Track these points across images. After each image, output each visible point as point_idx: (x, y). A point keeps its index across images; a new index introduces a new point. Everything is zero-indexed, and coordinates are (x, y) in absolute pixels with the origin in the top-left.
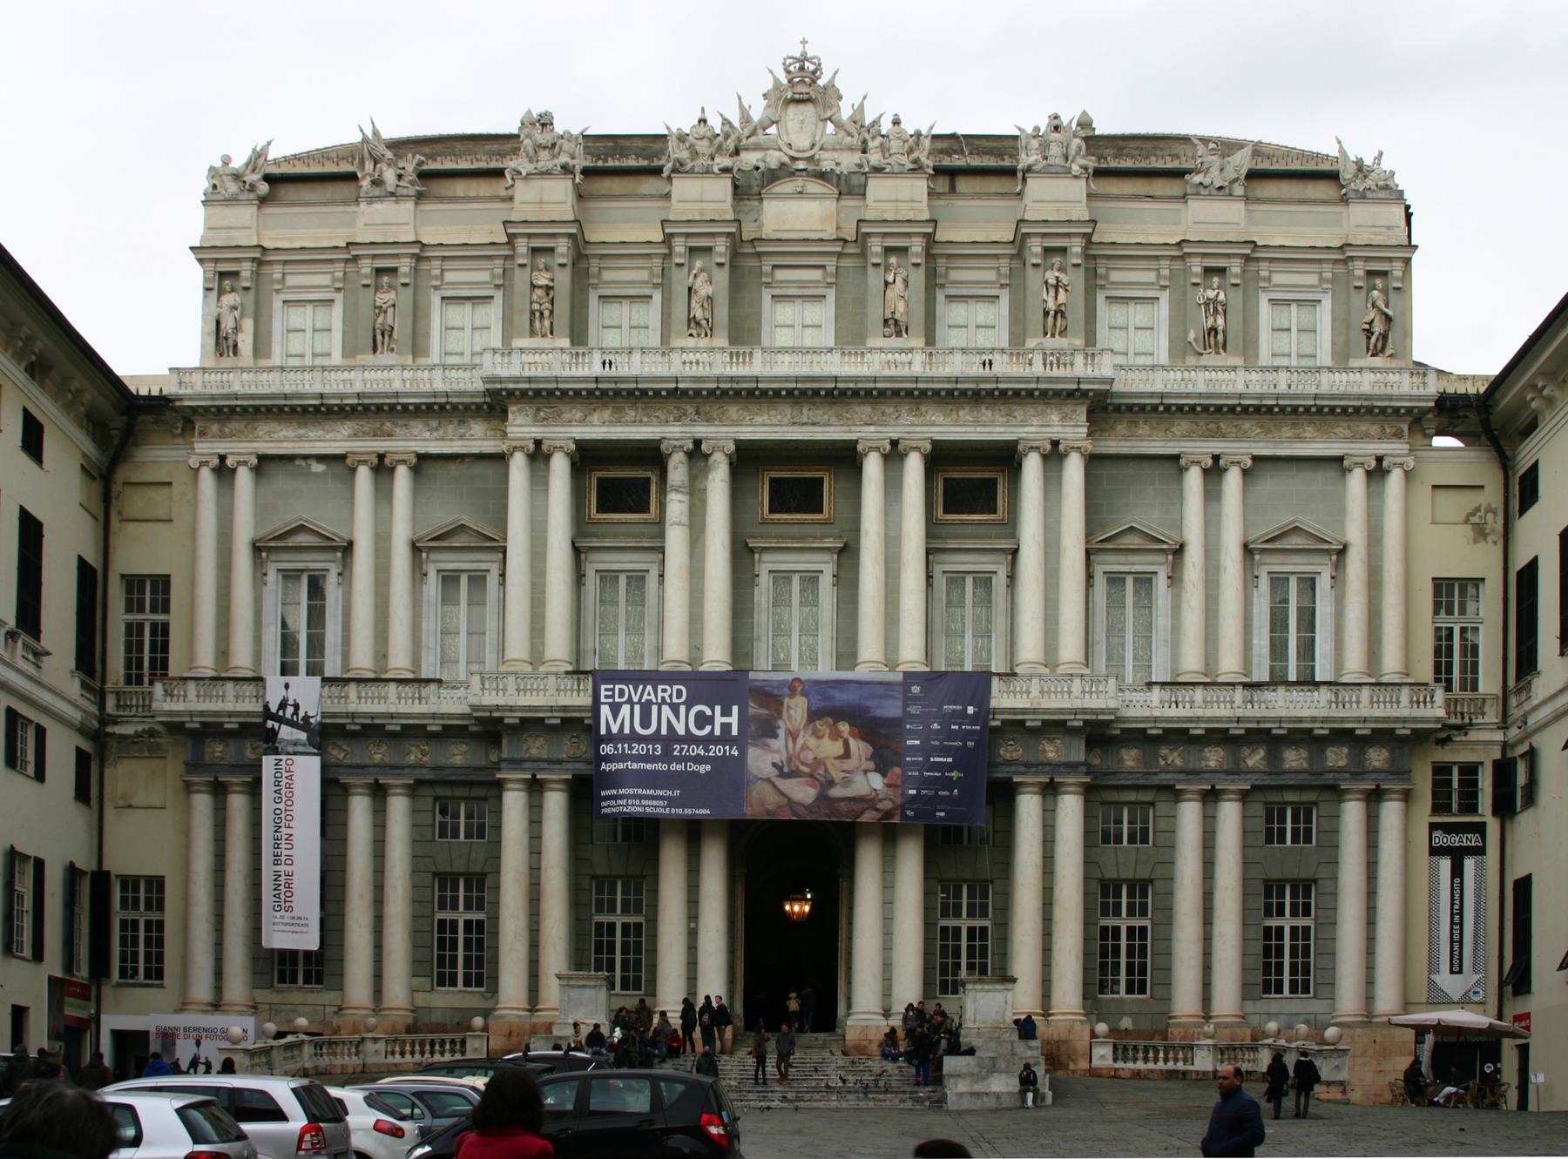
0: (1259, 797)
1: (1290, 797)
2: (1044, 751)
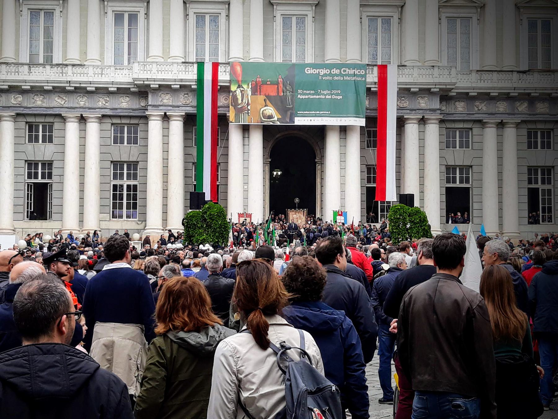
0: (524, 126)
1: (540, 126)
2: (419, 103)
